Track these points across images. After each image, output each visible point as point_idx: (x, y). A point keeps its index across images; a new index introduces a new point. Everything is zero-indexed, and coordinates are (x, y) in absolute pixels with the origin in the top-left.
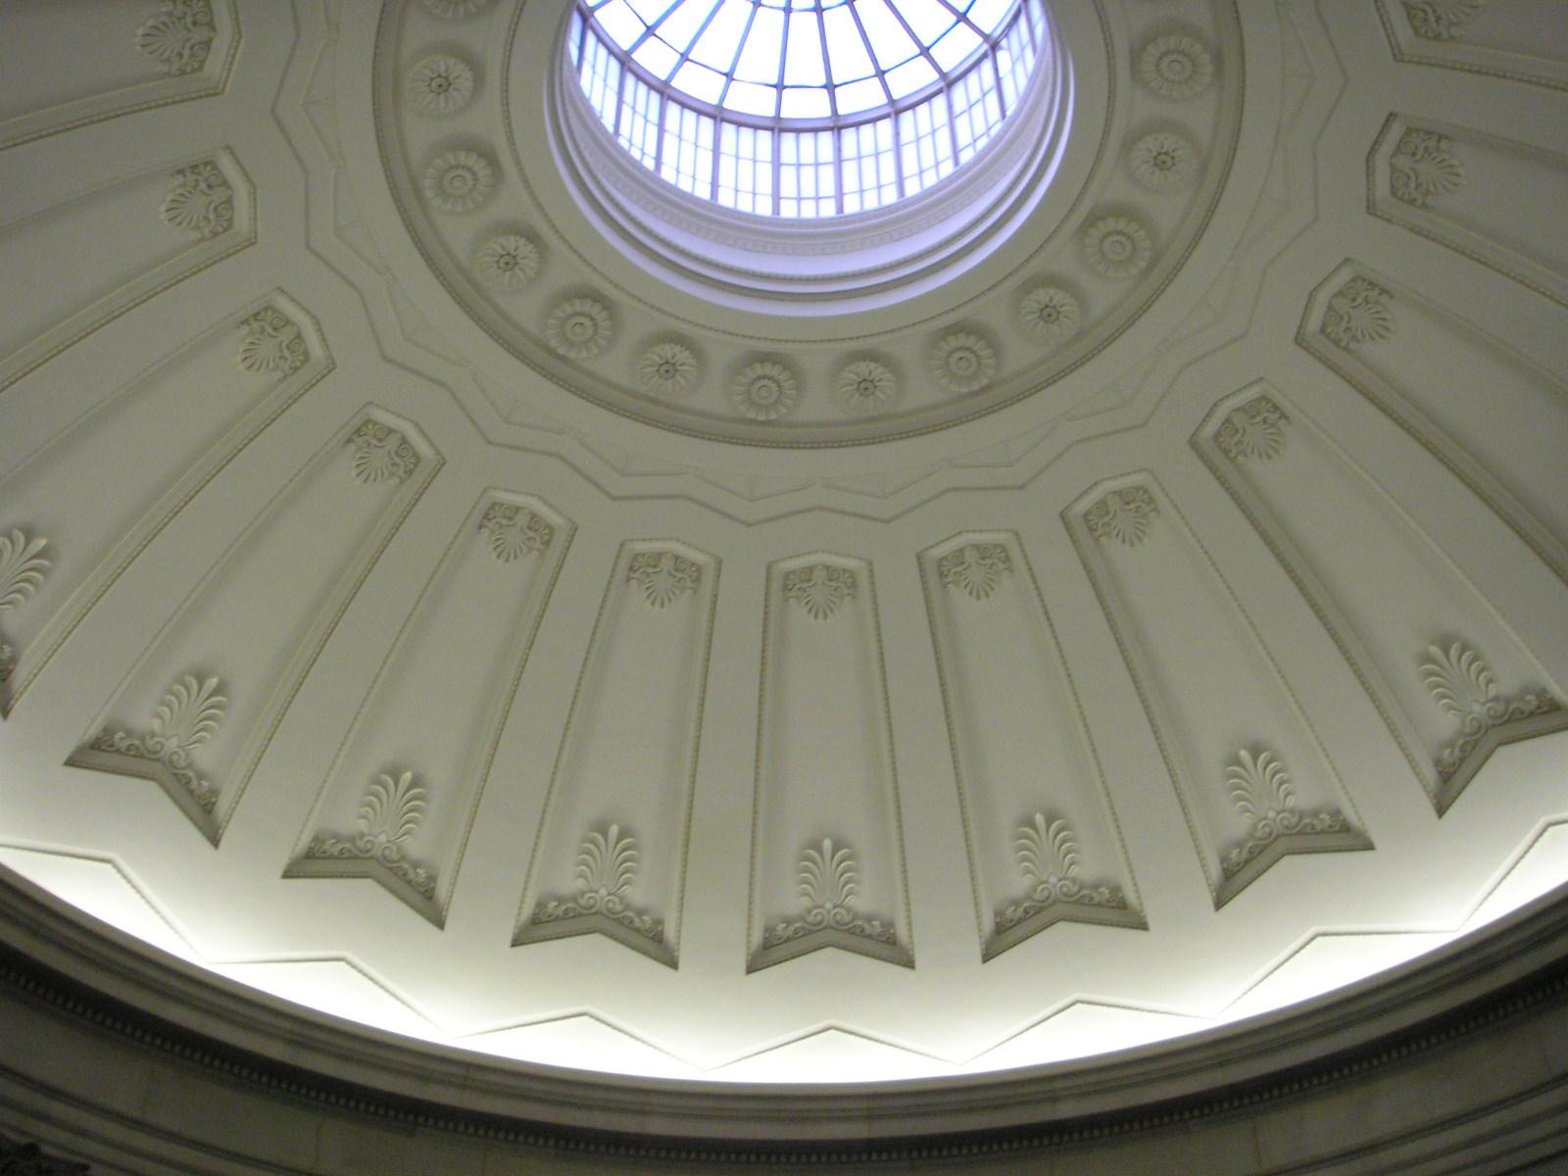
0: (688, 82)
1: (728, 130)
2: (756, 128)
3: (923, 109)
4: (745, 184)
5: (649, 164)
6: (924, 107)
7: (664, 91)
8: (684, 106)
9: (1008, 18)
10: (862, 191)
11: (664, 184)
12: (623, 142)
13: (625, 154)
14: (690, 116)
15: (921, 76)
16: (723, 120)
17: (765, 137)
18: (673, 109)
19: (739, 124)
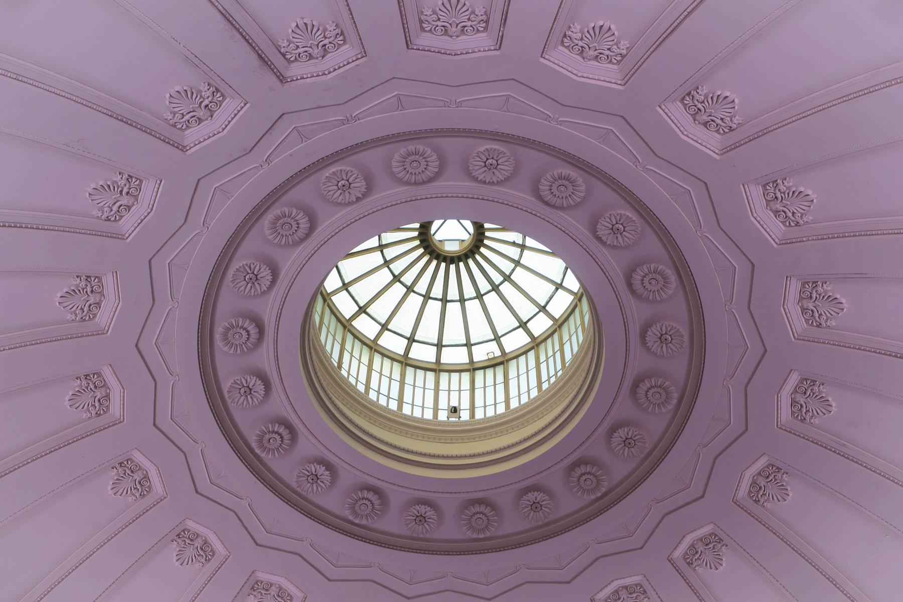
0: (389, 342)
1: (410, 371)
2: (426, 369)
3: (522, 359)
4: (418, 401)
5: (361, 388)
6: (523, 357)
7: (373, 347)
8: (383, 355)
9: (569, 310)
10: (485, 407)
11: (371, 402)
12: (344, 373)
13: (346, 381)
14: (387, 363)
15: (518, 340)
16: (407, 365)
17: (431, 376)
18: (377, 359)
19: (416, 367)
